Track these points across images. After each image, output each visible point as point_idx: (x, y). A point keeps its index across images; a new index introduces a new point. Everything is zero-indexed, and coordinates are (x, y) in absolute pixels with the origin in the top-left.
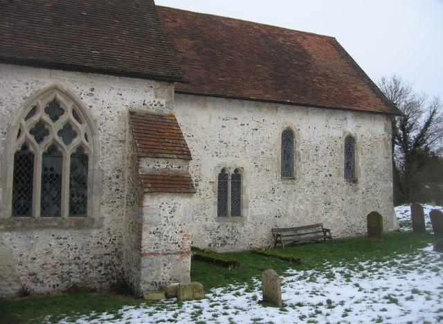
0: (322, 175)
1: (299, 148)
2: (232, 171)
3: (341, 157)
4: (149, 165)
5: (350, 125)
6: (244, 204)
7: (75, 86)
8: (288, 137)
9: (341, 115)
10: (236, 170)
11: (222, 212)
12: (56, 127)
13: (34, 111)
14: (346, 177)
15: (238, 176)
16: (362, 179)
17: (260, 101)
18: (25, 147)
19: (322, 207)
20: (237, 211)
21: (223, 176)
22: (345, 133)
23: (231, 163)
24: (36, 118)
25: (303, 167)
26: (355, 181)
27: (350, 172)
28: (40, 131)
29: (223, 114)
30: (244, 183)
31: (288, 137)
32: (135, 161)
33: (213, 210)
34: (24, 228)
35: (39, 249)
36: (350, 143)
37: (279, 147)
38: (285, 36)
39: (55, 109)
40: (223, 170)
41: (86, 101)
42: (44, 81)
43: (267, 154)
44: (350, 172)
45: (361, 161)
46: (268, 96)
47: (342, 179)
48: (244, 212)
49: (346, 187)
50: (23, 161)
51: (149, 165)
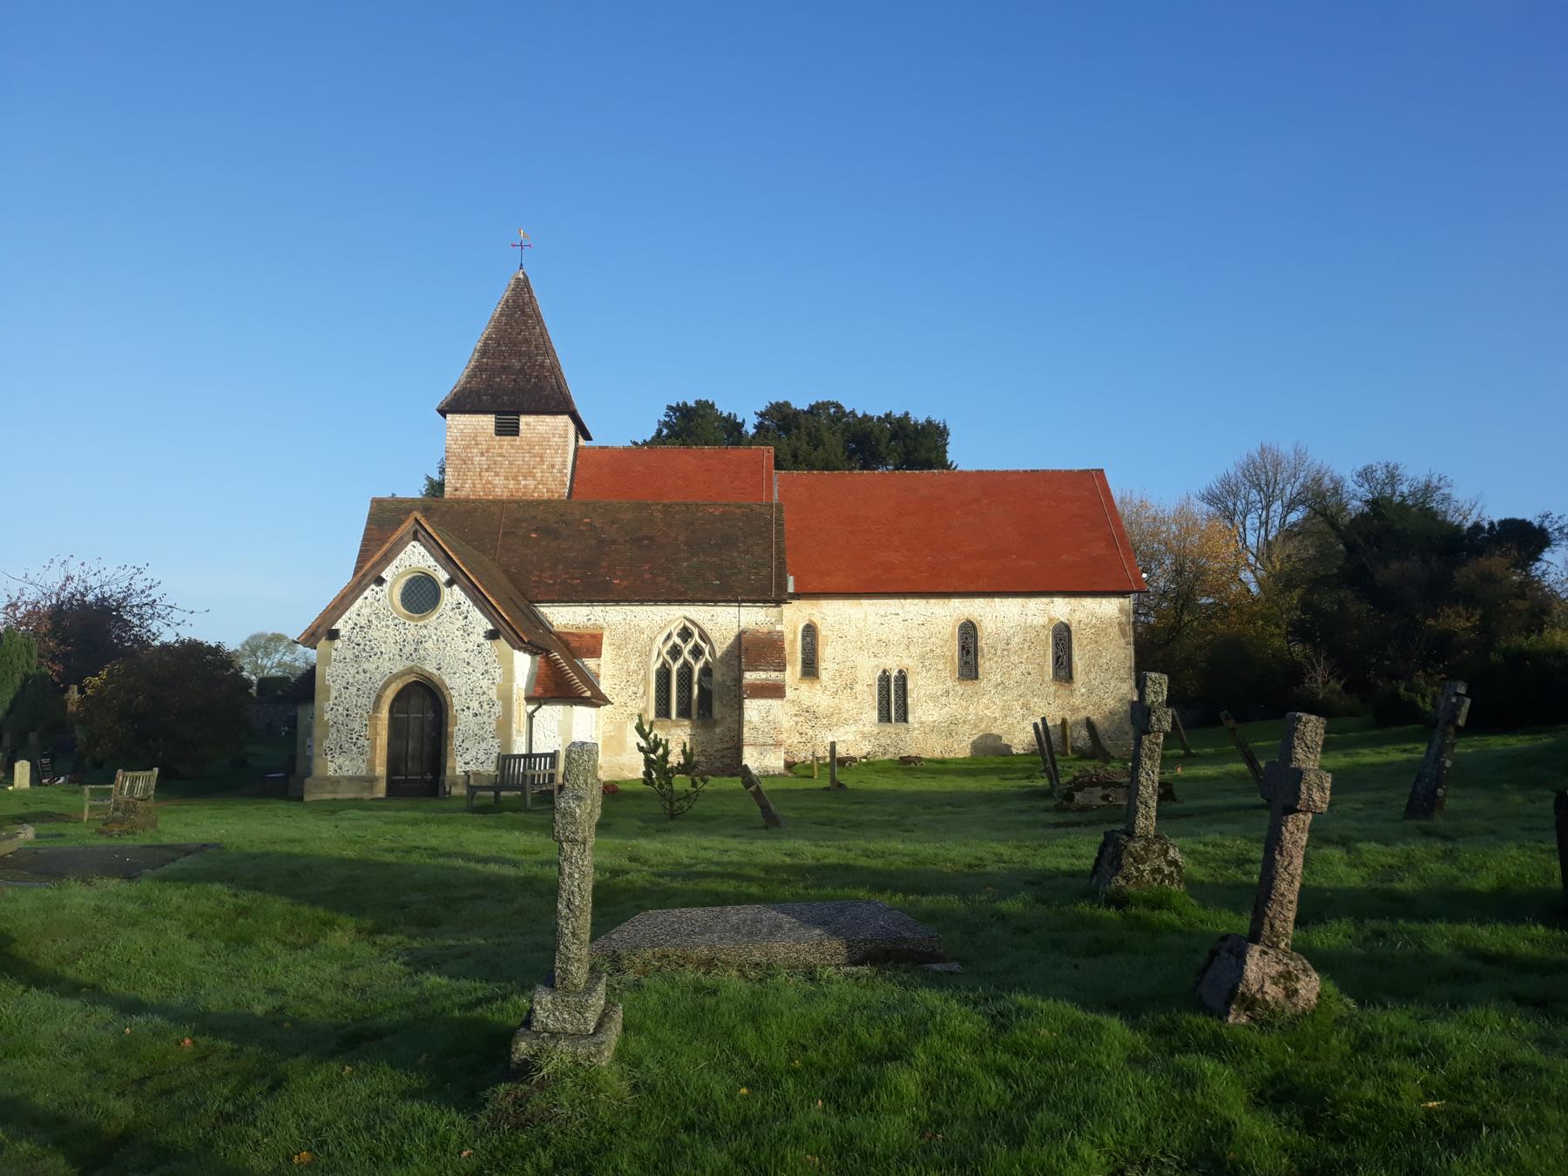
0: (1017, 673)
2: (894, 673)
5: (1061, 609)
7: (700, 614)
10: (900, 672)
11: (885, 716)
12: (687, 649)
13: (669, 636)
14: (1057, 677)
15: (902, 678)
18: (663, 665)
20: (903, 716)
21: (884, 679)
22: (1051, 620)
23: (893, 666)
24: (671, 643)
25: (985, 665)
27: (1063, 668)
28: (675, 652)
30: (910, 686)
33: (875, 715)
36: (1062, 636)
39: (685, 634)
40: (884, 672)
41: (707, 627)
42: (675, 615)
44: (1063, 668)
48: (910, 718)
49: (1052, 689)
50: (663, 675)
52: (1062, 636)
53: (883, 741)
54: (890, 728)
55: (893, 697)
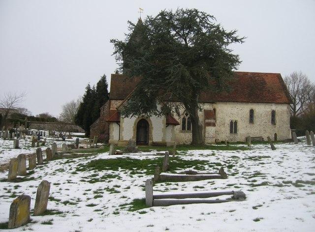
1: (255, 114)
3: (270, 117)
4: (207, 121)
5: (274, 107)
6: (238, 130)
8: (252, 112)
9: (270, 104)
11: (231, 132)
15: (236, 123)
16: (277, 124)
17: (242, 102)
19: (263, 132)
20: (236, 132)
21: (232, 122)
23: (234, 119)
25: (256, 120)
26: (275, 124)
27: (273, 121)
29: (232, 106)
31: (252, 112)
32: (205, 120)
33: (228, 131)
34: (184, 132)
35: (187, 136)
36: (273, 113)
37: (249, 114)
38: (259, 76)
43: (245, 116)
44: (273, 121)
45: (277, 118)
46: (245, 100)
47: (270, 123)
48: (238, 133)
51: (207, 121)
52: (273, 113)
53: (231, 138)
54: (233, 135)
55: (234, 126)
